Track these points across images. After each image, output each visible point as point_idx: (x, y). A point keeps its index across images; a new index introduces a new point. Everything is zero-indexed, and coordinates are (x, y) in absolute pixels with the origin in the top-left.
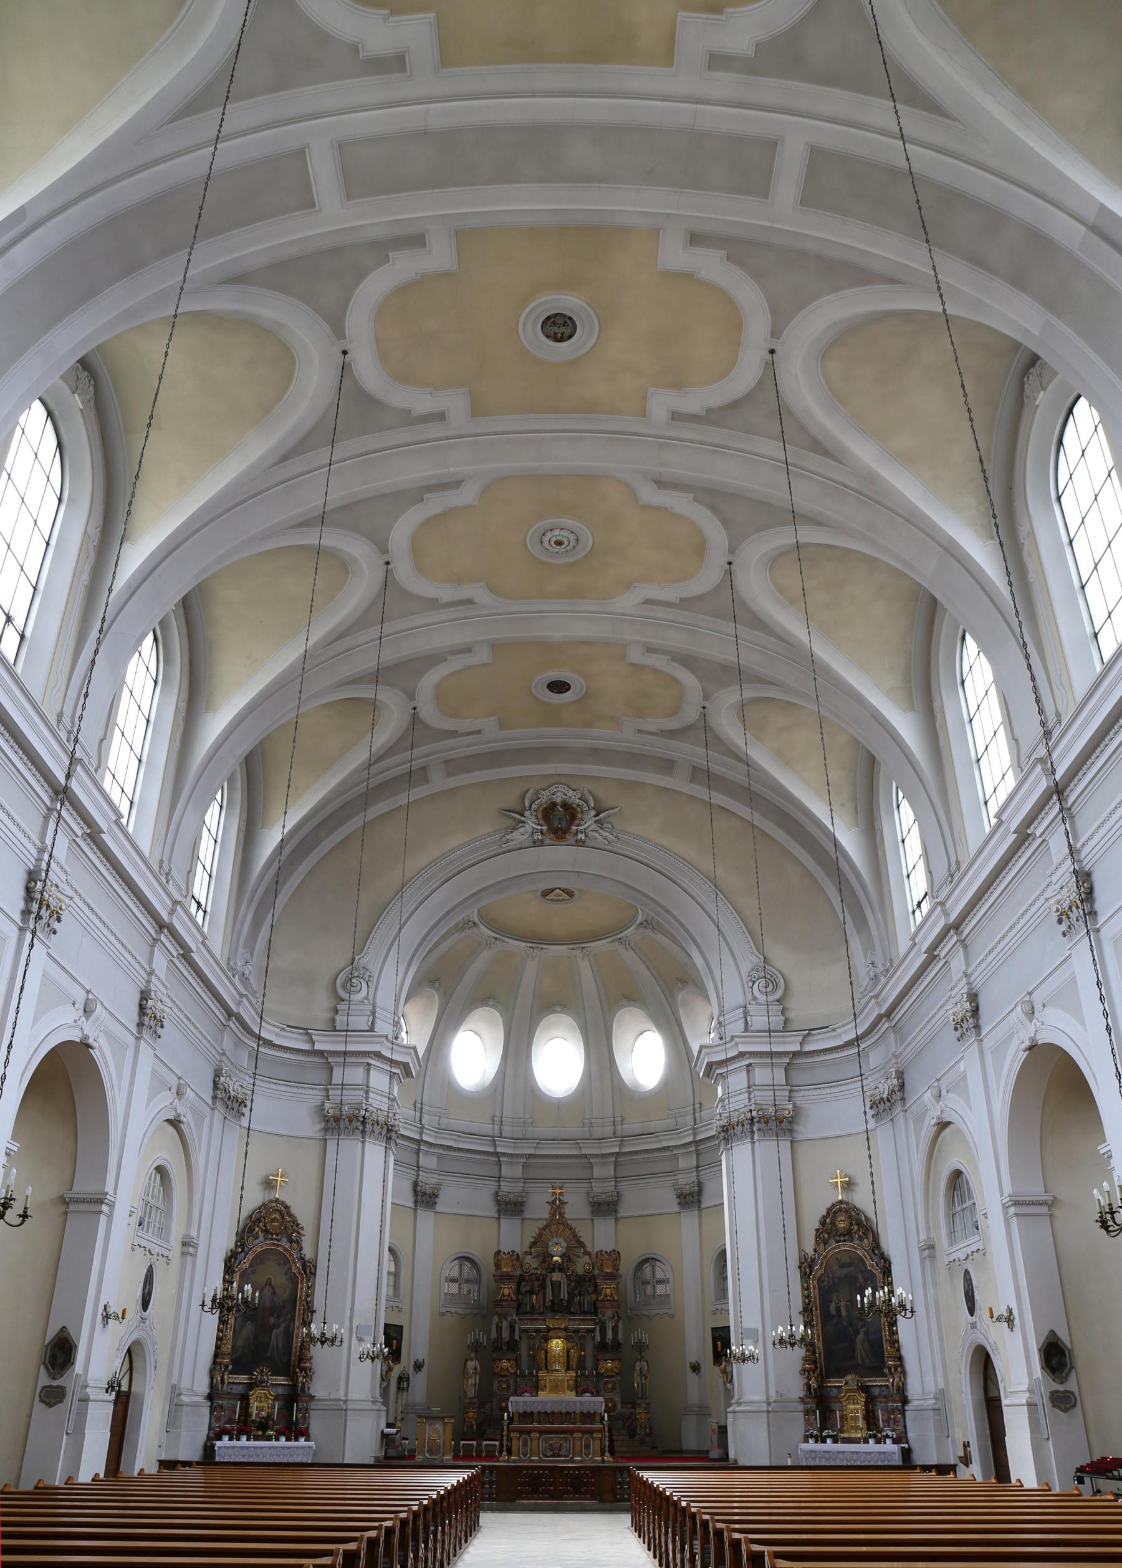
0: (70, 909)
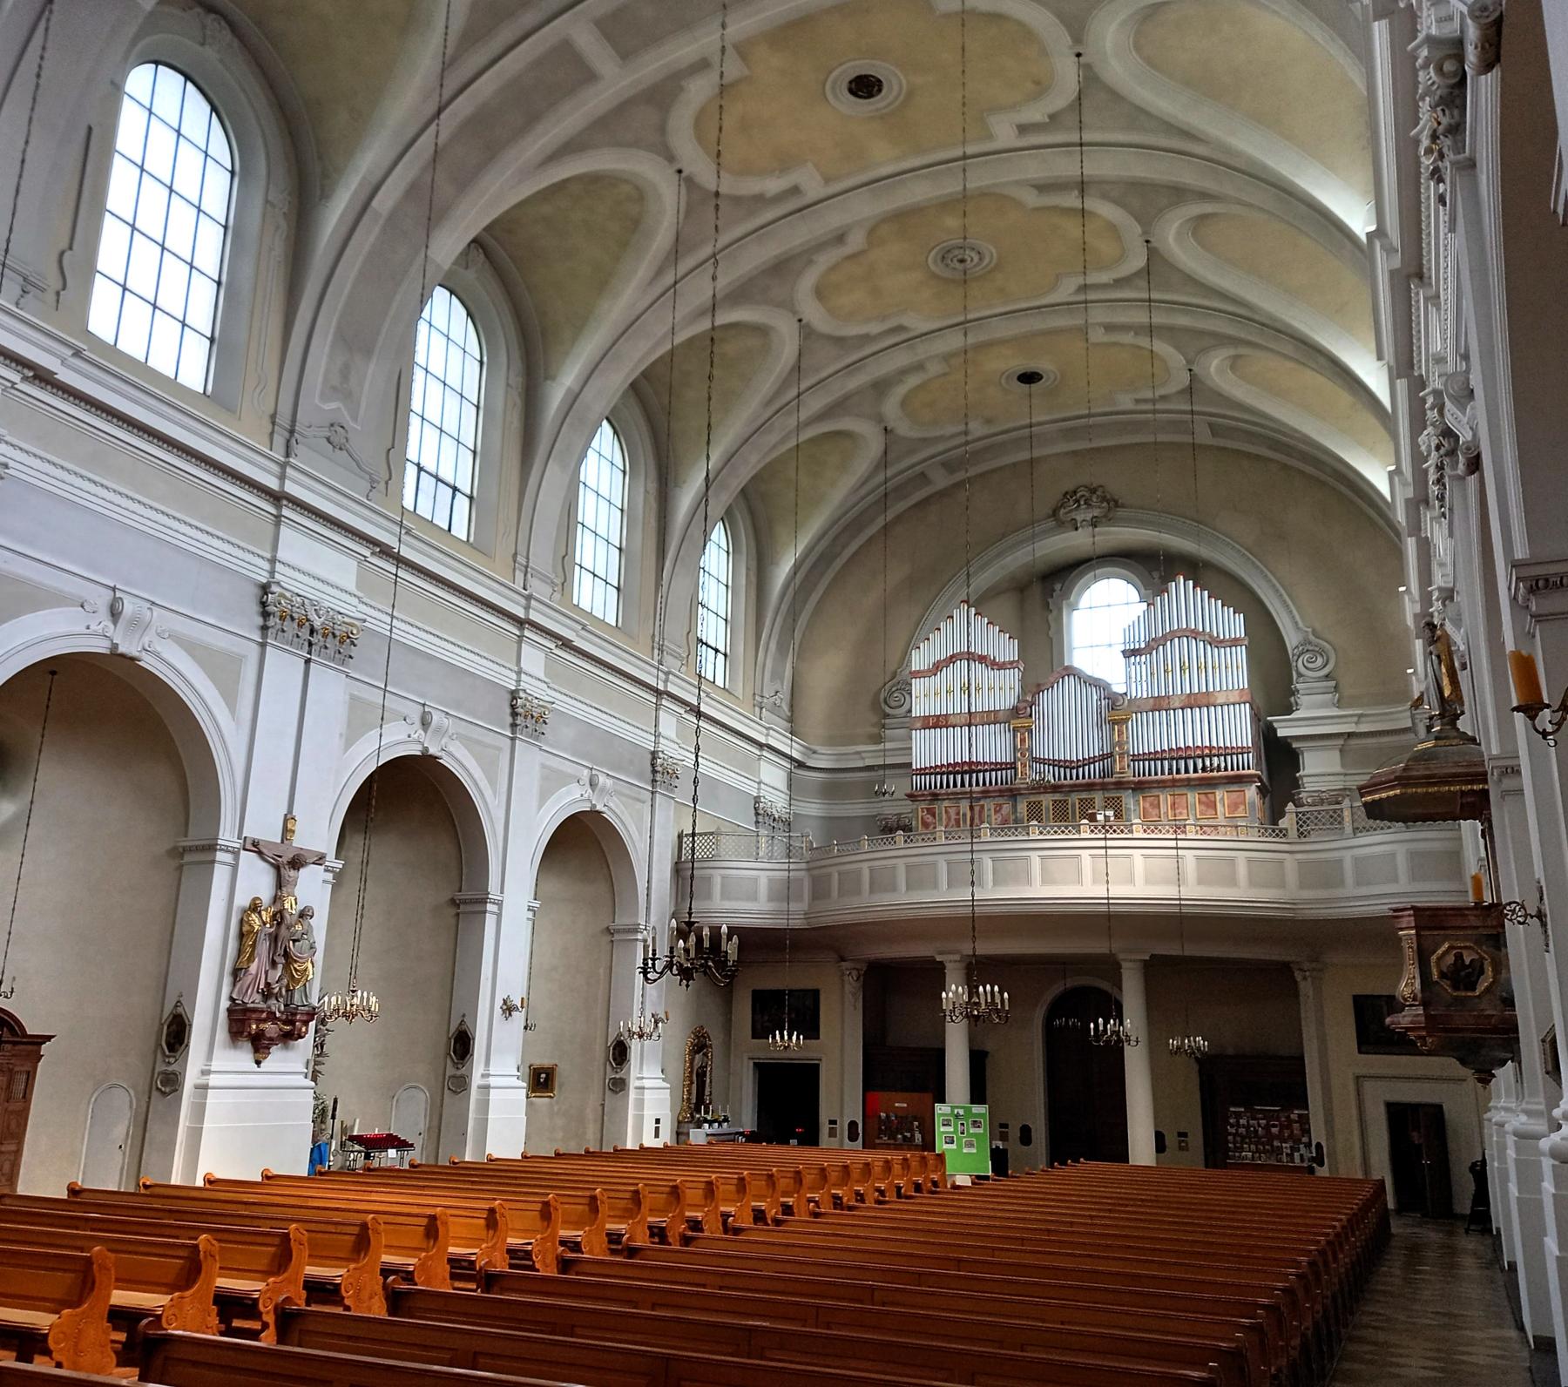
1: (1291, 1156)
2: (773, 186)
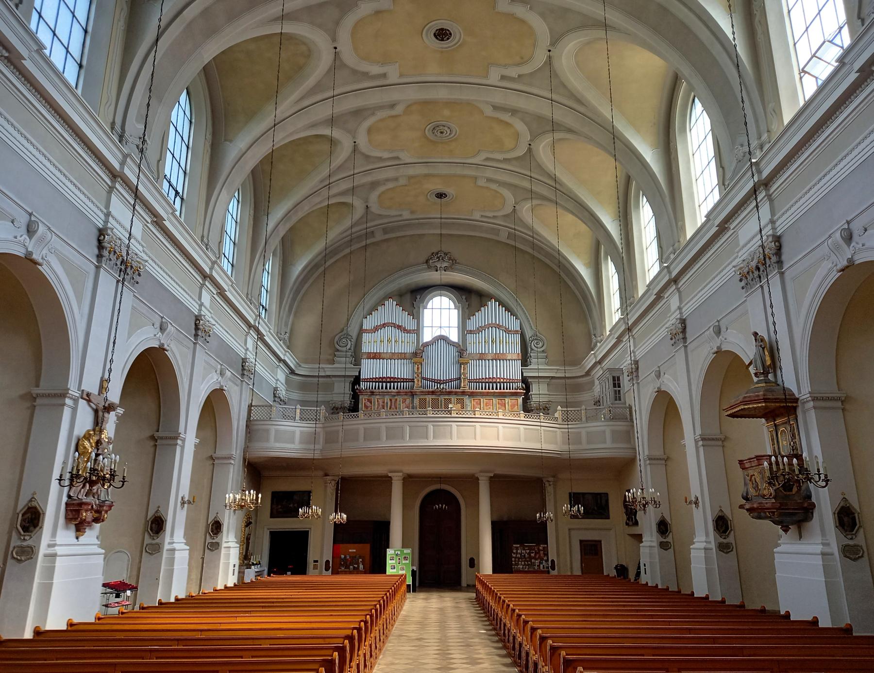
0: (214, 330)
1: (539, 566)
2: (375, 70)
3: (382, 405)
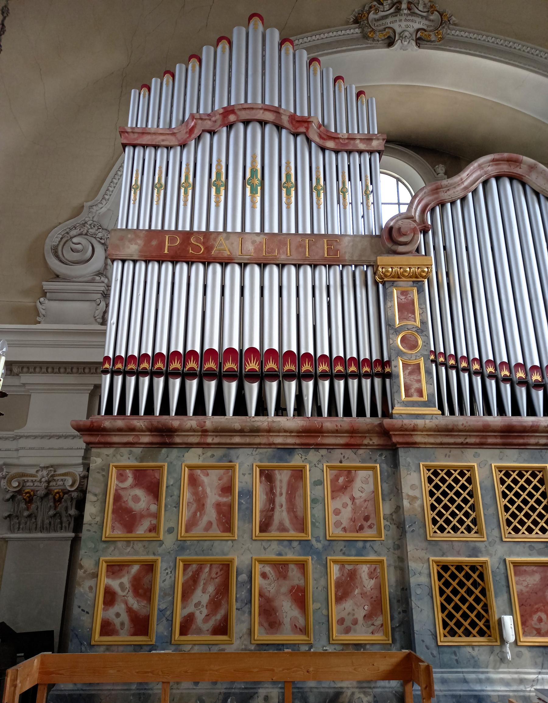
3: (218, 506)
